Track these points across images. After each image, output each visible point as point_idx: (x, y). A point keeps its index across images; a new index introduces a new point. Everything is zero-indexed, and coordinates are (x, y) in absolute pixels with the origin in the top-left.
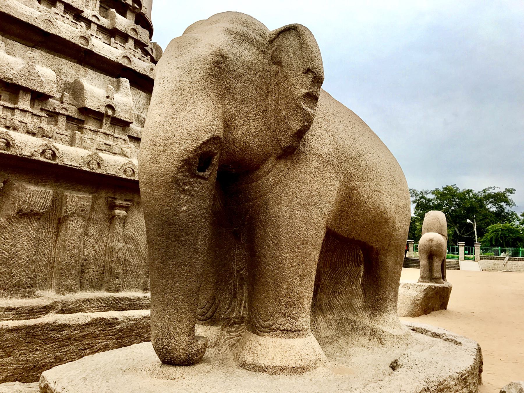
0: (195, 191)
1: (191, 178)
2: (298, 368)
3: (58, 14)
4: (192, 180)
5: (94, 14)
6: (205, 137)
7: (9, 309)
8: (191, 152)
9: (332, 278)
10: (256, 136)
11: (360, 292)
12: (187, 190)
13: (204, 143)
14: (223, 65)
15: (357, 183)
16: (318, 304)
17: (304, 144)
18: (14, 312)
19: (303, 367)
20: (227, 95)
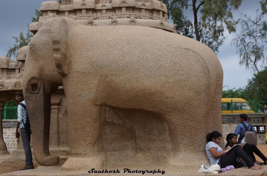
0: (33, 99)
1: (31, 94)
2: (69, 169)
3: (81, 16)
4: (31, 95)
5: (103, 5)
6: (29, 78)
7: (64, 151)
8: (26, 85)
9: (145, 132)
10: (53, 71)
11: (169, 139)
12: (31, 99)
13: (29, 81)
14: (33, 48)
15: (112, 78)
16: (138, 147)
17: (71, 68)
18: (65, 152)
19: (71, 169)
20: (38, 59)
